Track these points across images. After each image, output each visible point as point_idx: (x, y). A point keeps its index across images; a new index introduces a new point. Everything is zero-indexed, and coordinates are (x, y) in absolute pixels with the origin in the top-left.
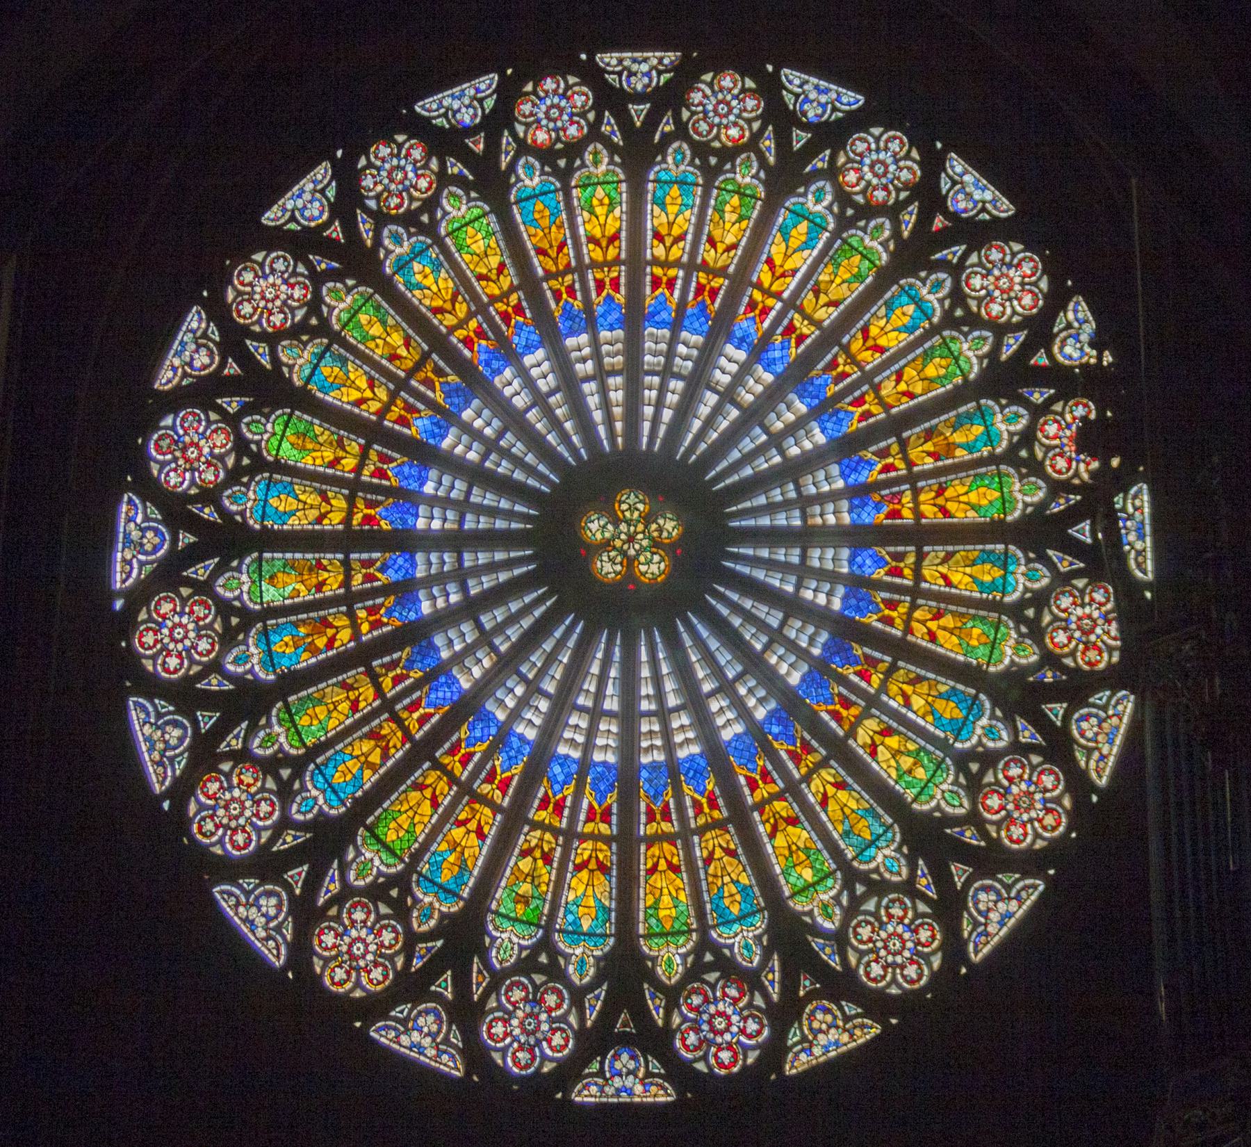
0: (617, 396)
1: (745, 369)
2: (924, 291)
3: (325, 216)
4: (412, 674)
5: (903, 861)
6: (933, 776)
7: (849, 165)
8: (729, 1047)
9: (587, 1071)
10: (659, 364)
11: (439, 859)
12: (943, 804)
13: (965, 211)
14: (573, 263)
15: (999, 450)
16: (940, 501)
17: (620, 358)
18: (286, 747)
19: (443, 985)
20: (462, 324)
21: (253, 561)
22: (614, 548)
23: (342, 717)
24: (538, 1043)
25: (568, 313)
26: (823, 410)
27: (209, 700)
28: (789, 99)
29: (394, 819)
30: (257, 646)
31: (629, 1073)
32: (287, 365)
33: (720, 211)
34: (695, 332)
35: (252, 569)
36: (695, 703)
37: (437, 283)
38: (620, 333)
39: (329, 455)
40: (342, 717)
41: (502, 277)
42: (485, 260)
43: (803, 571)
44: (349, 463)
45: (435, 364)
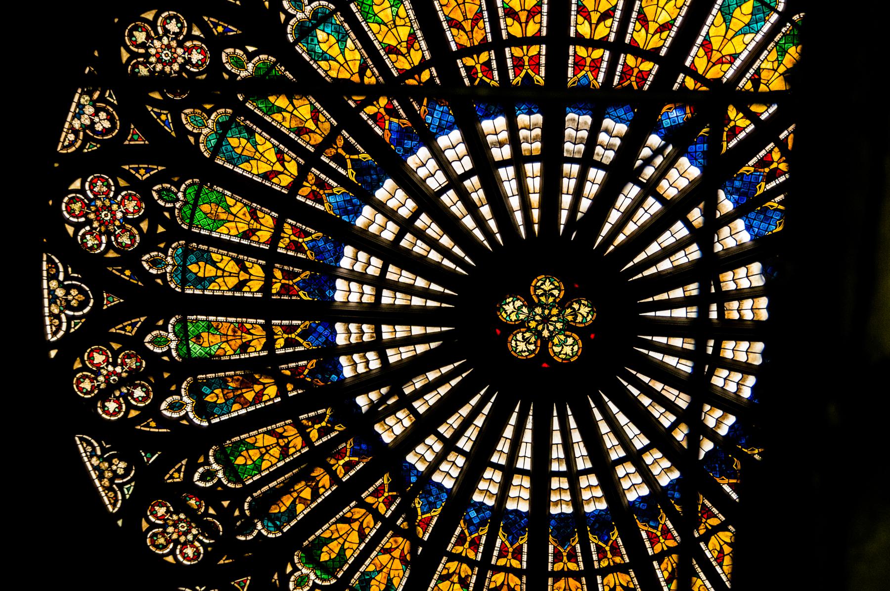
0: (534, 184)
4: (336, 428)
10: (579, 152)
17: (537, 145)
21: (177, 321)
22: (529, 329)
23: (274, 460)
27: (151, 442)
30: (189, 396)
32: (192, 133)
34: (619, 120)
35: (177, 328)
37: (342, 53)
38: (538, 118)
39: (243, 227)
40: (274, 460)
41: (412, 50)
42: (394, 30)
44: (265, 235)
45: (345, 140)
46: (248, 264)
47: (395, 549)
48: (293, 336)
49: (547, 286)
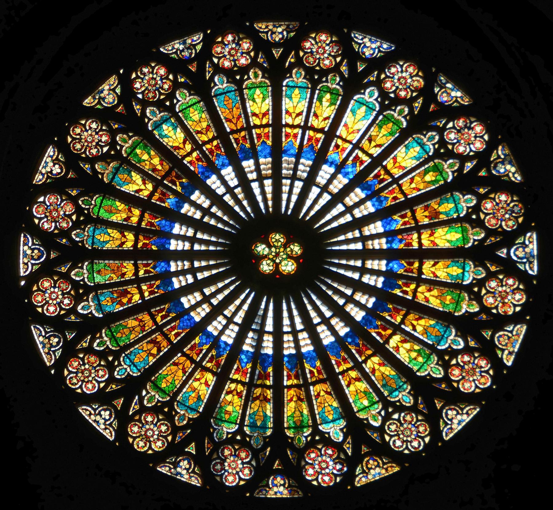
0: (269, 189)
1: (333, 177)
2: (425, 140)
3: (116, 102)
4: (170, 315)
5: (411, 398)
6: (427, 361)
7: (387, 79)
8: (328, 474)
9: (261, 484)
10: (290, 174)
11: (187, 395)
12: (431, 373)
13: (446, 102)
14: (245, 126)
15: (462, 215)
16: (432, 238)
18: (110, 347)
19: (191, 448)
20: (189, 154)
22: (269, 259)
23: (137, 334)
24: (237, 473)
25: (243, 149)
26: (373, 195)
27: (71, 326)
28: (356, 47)
29: (165, 378)
30: (93, 302)
31: (281, 485)
33: (320, 100)
34: (308, 159)
36: (310, 328)
37: (175, 134)
38: (270, 159)
39: (124, 216)
40: (137, 334)
41: (208, 133)
42: (200, 124)
43: (363, 270)
44: (135, 220)
46: (126, 234)
47: (202, 378)
48: (148, 268)
49: (278, 237)
